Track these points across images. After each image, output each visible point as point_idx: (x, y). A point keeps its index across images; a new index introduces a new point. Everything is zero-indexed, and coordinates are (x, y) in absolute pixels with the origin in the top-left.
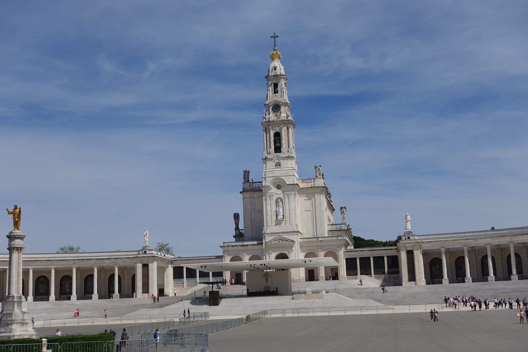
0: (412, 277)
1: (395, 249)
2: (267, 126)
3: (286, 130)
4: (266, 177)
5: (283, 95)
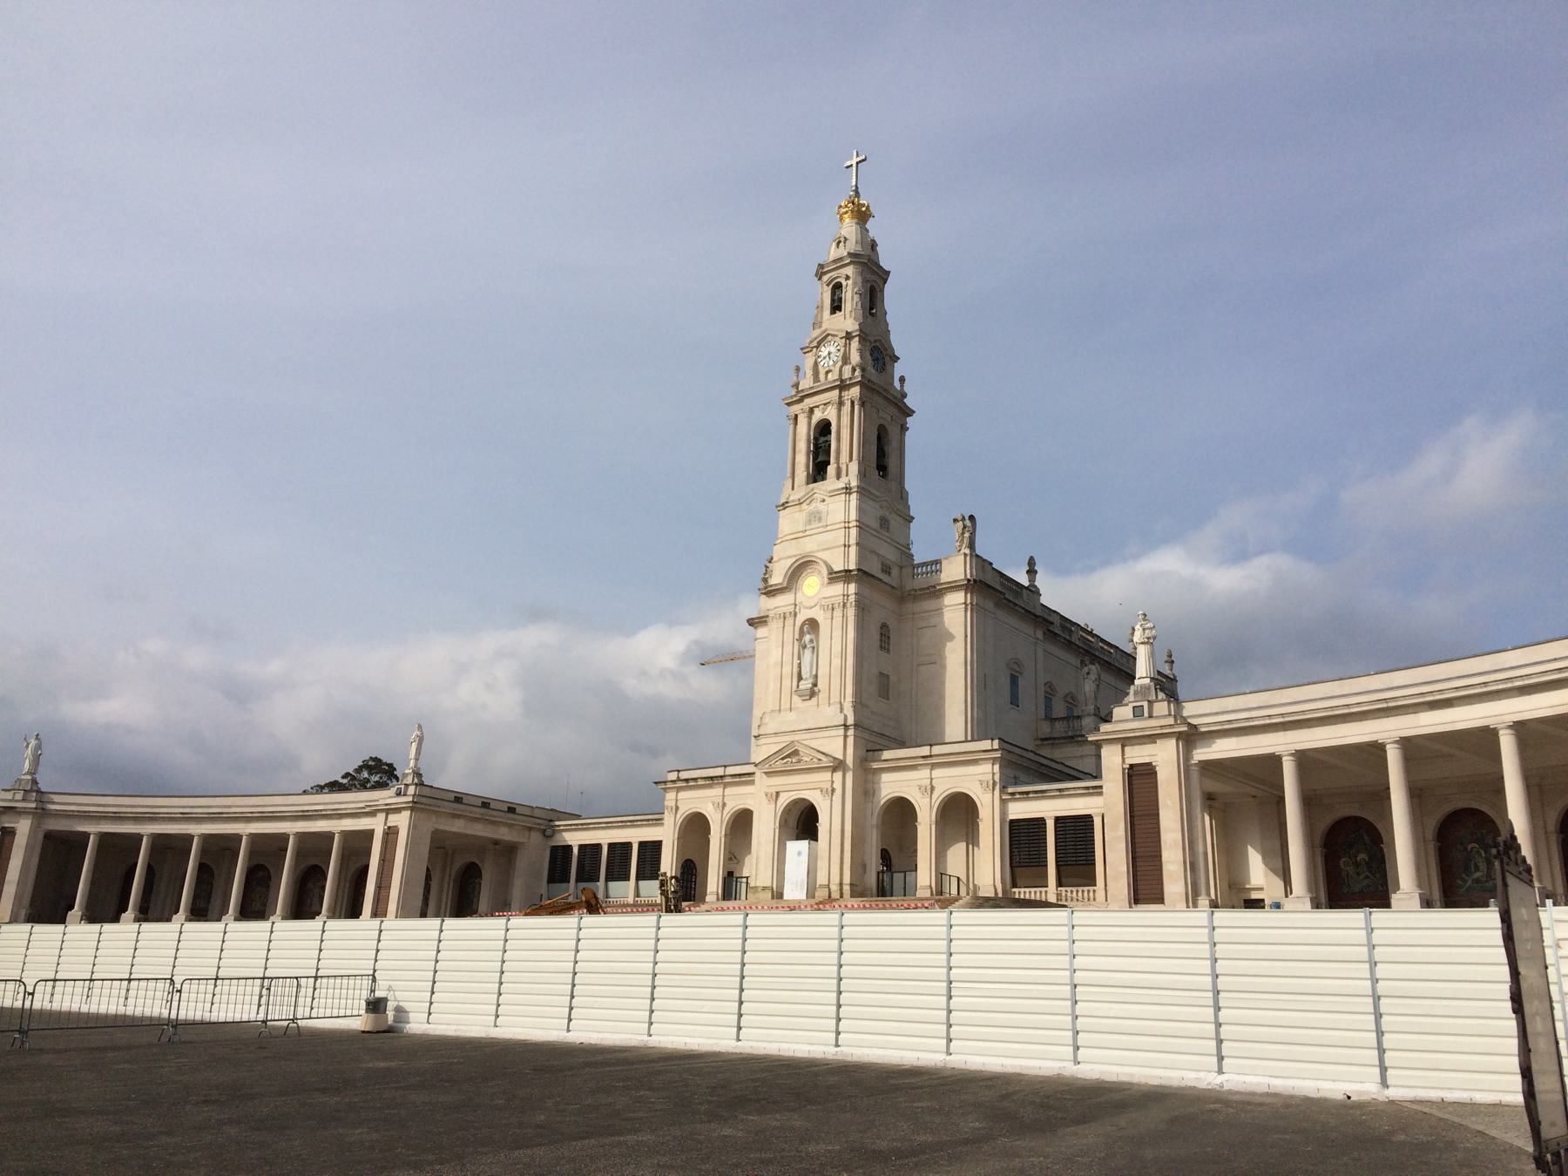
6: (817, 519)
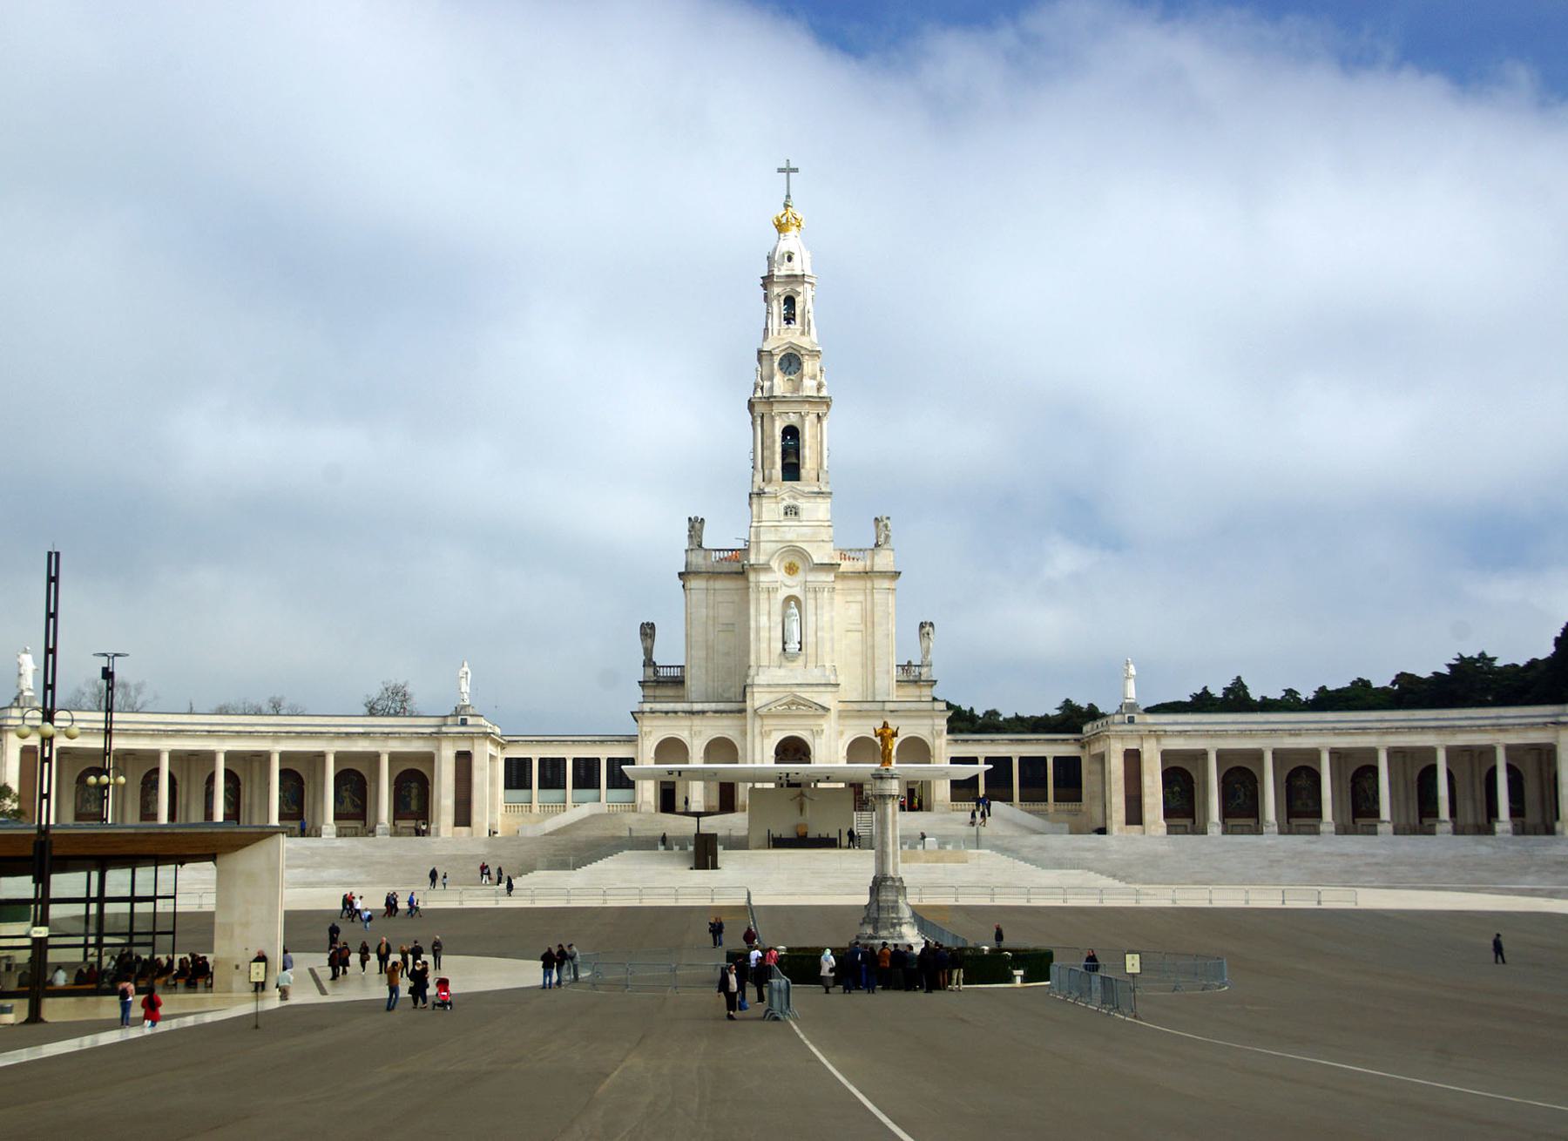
0: (1135, 815)
1: (1075, 740)
2: (760, 406)
3: (816, 420)
4: (760, 542)
5: (809, 329)
6: (793, 513)
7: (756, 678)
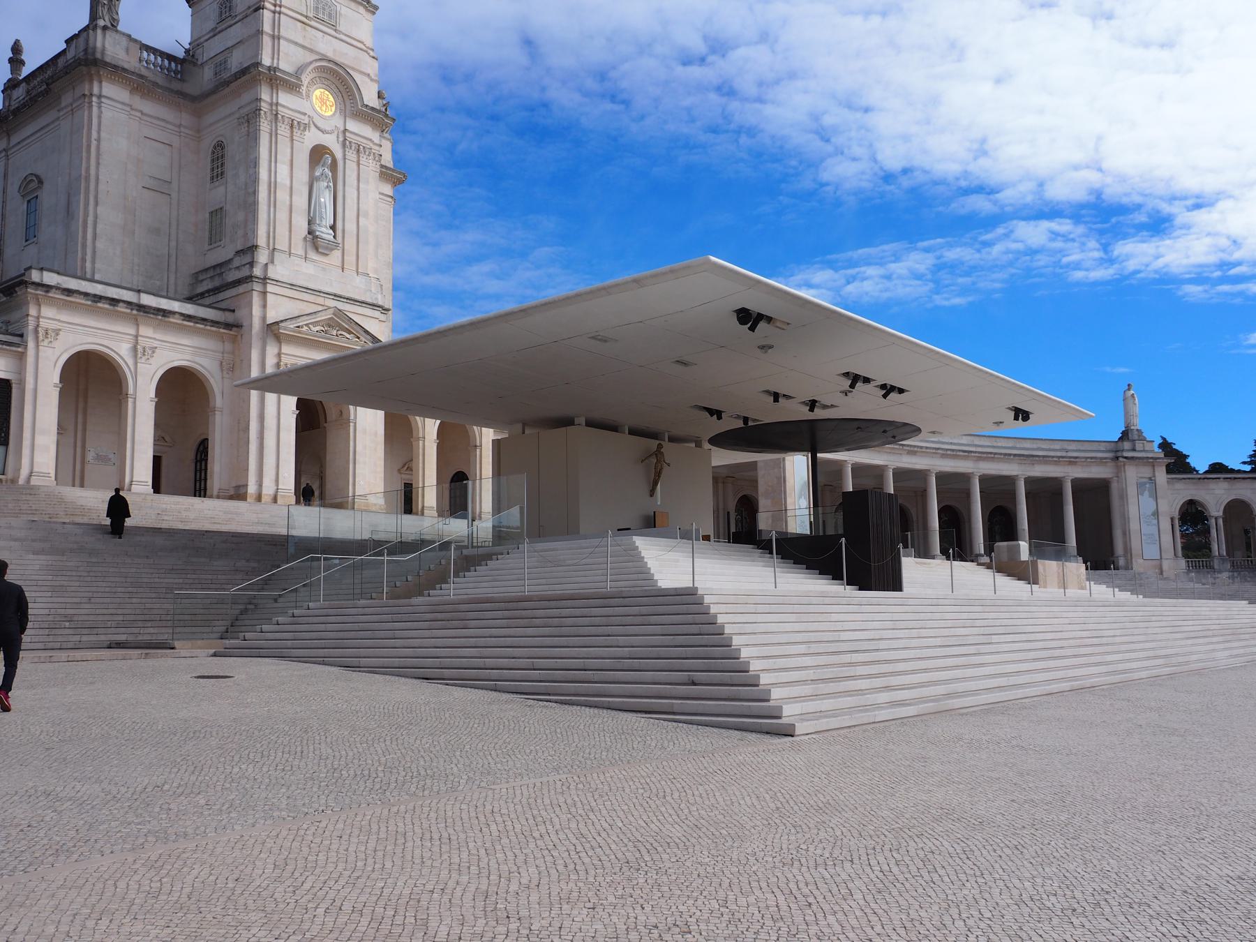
7: (270, 267)
